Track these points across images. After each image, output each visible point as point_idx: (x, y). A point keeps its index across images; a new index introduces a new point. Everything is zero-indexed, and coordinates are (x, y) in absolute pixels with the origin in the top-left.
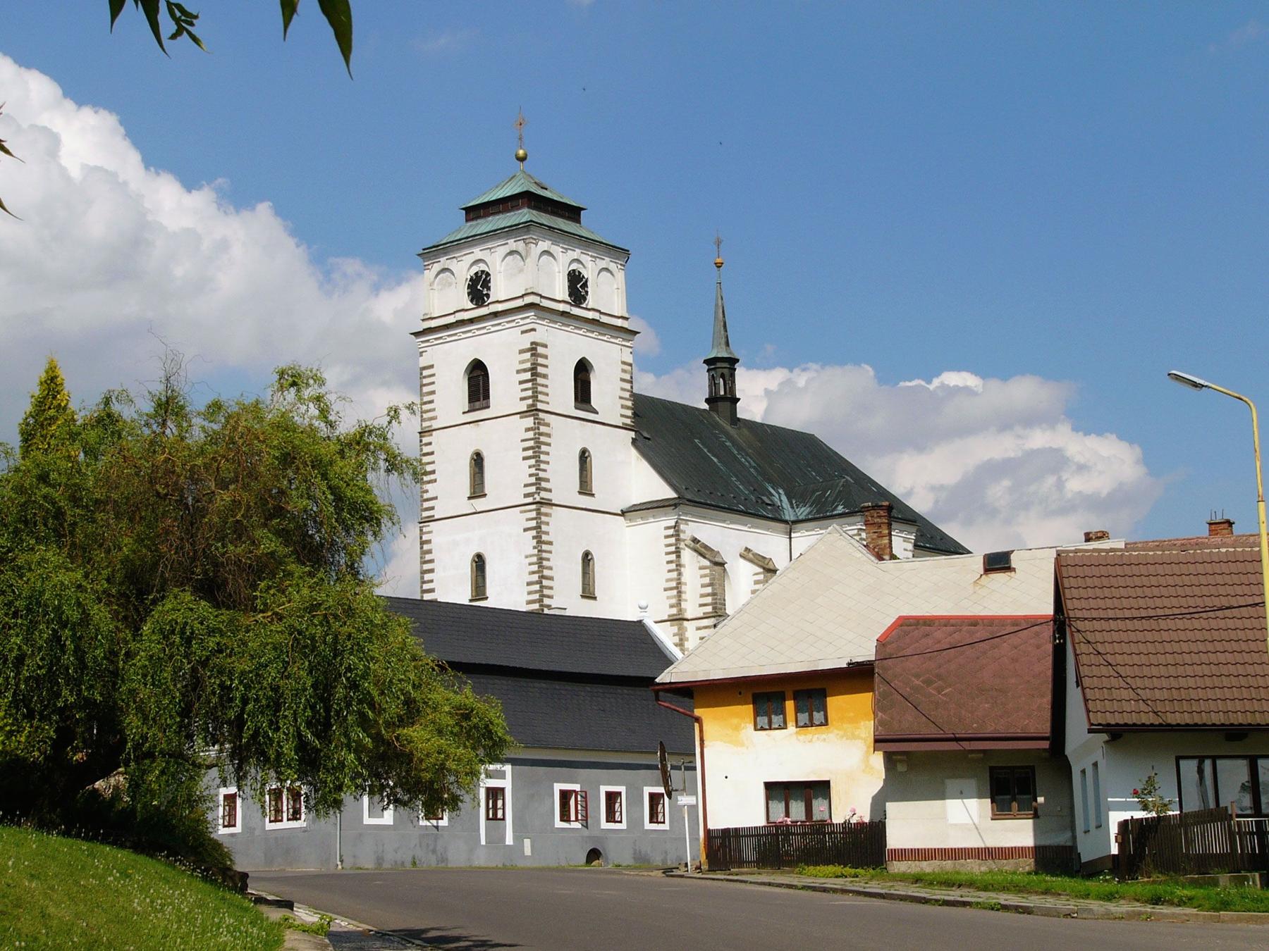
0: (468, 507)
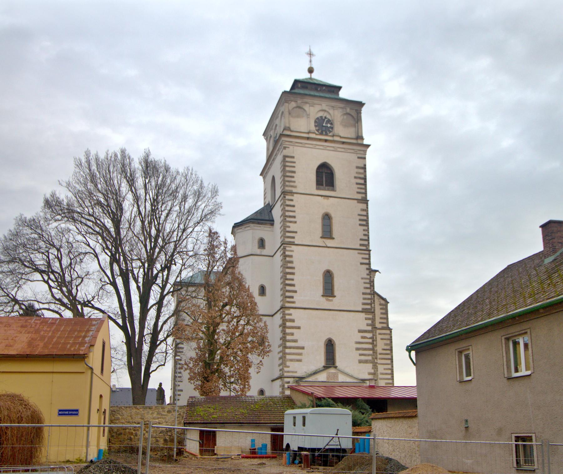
0: (320, 242)
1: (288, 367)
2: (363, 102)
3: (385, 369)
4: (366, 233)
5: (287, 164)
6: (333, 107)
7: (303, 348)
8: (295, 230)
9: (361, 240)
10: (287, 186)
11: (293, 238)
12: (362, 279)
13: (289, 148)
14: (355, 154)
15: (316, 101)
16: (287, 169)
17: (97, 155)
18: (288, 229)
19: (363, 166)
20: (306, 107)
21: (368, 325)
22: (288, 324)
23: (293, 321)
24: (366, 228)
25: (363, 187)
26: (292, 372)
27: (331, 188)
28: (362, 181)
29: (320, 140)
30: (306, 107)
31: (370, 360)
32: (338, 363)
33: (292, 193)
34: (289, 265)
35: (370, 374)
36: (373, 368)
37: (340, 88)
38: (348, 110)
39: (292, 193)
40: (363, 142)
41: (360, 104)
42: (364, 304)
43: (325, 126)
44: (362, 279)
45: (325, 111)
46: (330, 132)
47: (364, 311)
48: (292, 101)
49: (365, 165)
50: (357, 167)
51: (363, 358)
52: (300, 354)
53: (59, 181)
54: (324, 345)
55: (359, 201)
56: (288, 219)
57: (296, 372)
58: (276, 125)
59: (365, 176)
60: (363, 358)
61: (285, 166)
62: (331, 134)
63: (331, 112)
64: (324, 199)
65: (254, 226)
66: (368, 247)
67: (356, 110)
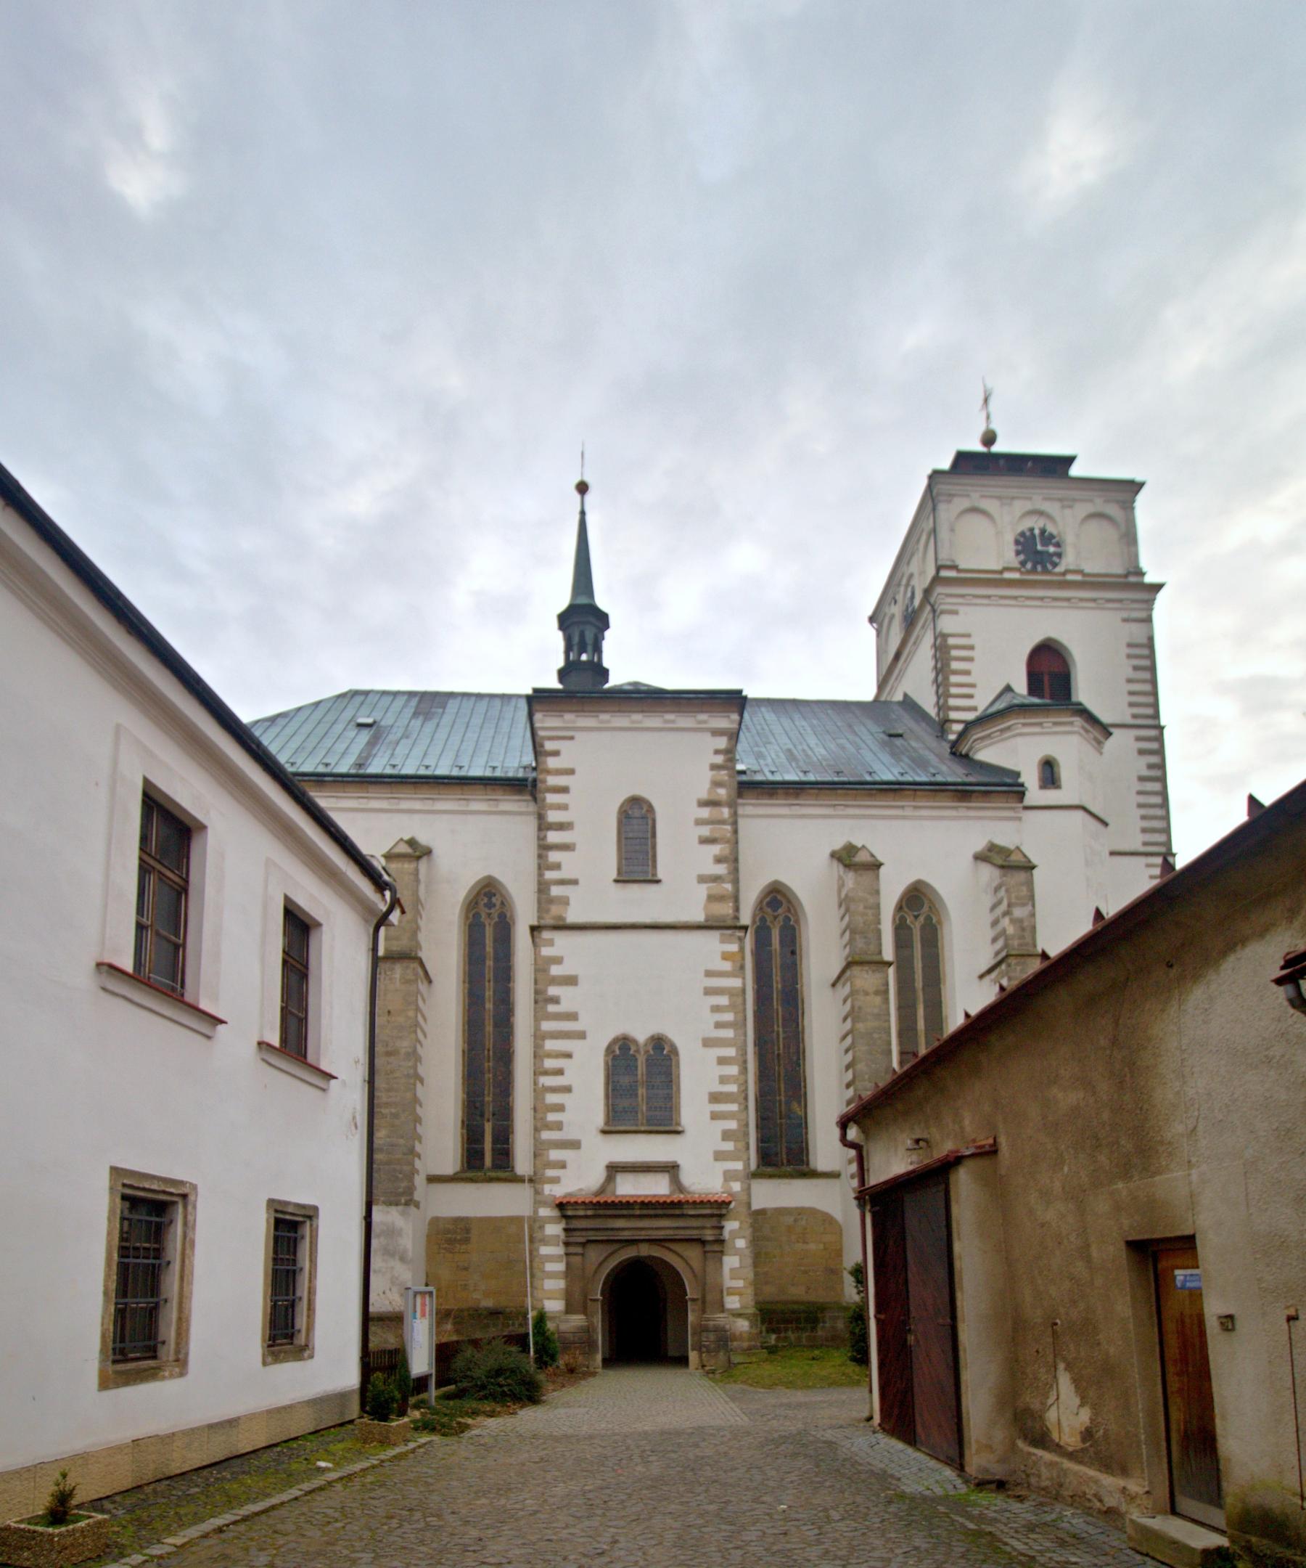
45: (1041, 513)
46: (1055, 565)
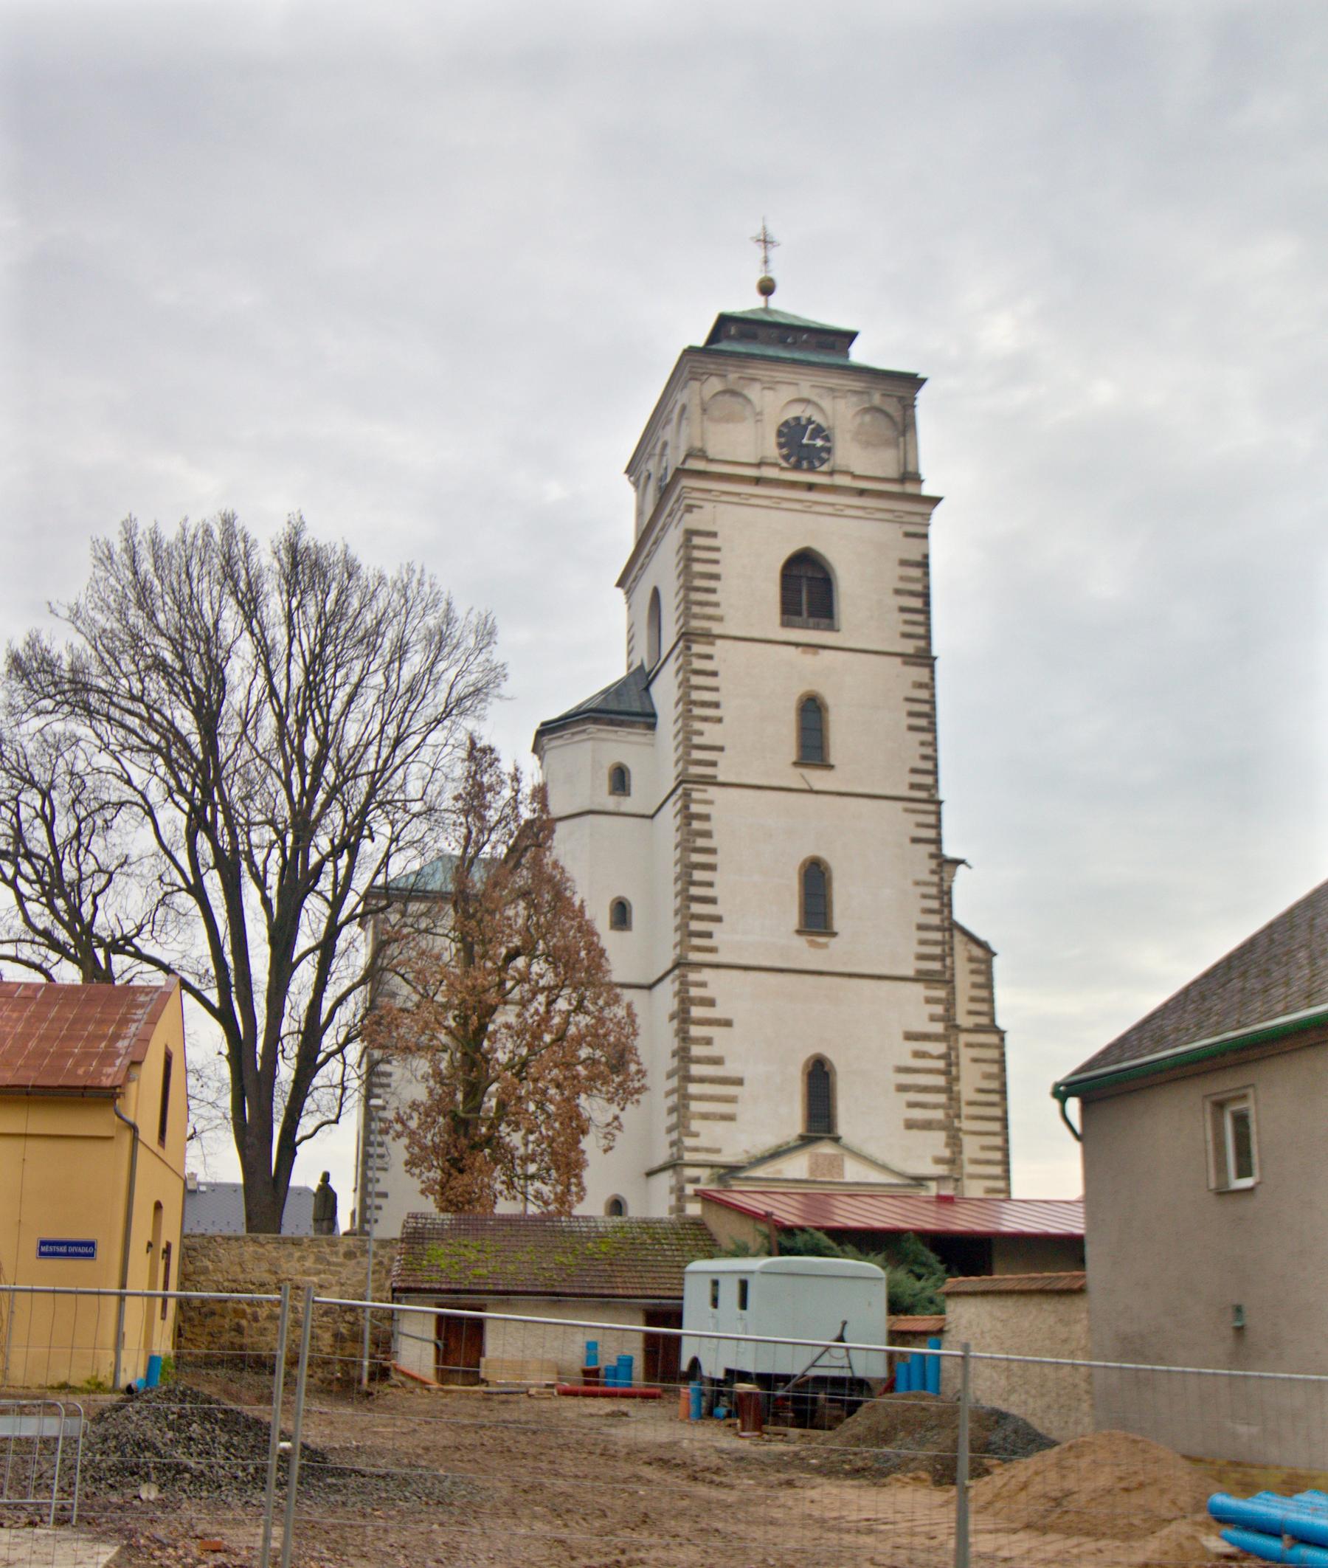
1: (696, 1135)
2: (921, 376)
3: (984, 1148)
4: (928, 751)
5: (696, 554)
6: (831, 389)
7: (739, 1082)
8: (718, 743)
9: (914, 771)
10: (695, 616)
11: (713, 764)
12: (917, 883)
13: (700, 507)
14: (898, 525)
15: (781, 374)
16: (697, 567)
17: (155, 532)
18: (697, 740)
19: (919, 558)
20: (754, 392)
21: (933, 1018)
22: (696, 1012)
23: (710, 1003)
24: (927, 737)
25: (920, 618)
26: (708, 1150)
27: (826, 621)
28: (917, 603)
29: (793, 485)
30: (754, 392)
31: (940, 1122)
32: (843, 1128)
33: (709, 637)
34: (701, 842)
35: (938, 1161)
36: (947, 1145)
37: (851, 336)
38: (877, 399)
39: (709, 637)
40: (920, 488)
41: (914, 382)
42: (922, 957)
43: (807, 446)
44: (917, 883)
45: (807, 401)
46: (823, 461)
47: (923, 977)
48: (711, 375)
49: (926, 557)
50: (904, 563)
51: (918, 1114)
52: (731, 1100)
53: (50, 604)
54: (803, 1073)
55: (908, 659)
56: (697, 711)
57: (718, 1151)
58: (665, 445)
59: (927, 587)
60: (918, 1114)
61: (689, 560)
62: (824, 468)
63: (826, 403)
64: (804, 652)
65: (599, 730)
66: (933, 792)
67: (901, 399)
